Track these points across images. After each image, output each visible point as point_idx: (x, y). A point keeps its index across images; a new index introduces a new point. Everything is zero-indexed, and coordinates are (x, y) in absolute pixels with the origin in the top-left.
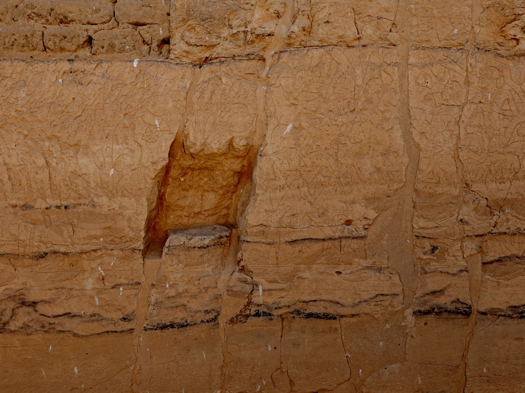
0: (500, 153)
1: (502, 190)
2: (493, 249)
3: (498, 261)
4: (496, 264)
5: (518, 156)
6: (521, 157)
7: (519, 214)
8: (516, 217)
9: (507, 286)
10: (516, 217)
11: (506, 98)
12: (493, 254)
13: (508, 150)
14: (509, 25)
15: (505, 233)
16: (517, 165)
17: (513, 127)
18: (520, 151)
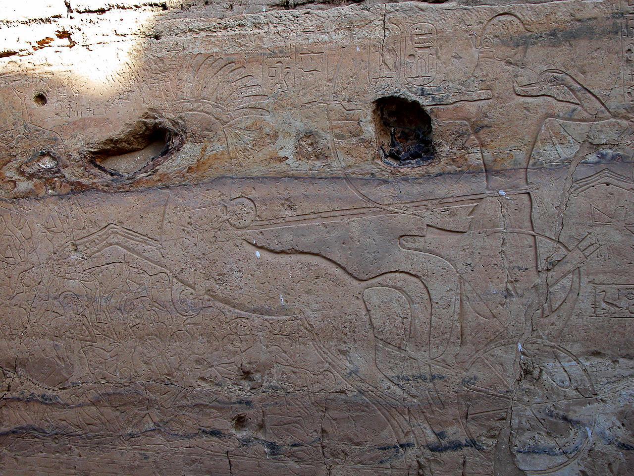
0: (6, 306)
1: (12, 348)
2: (8, 418)
3: (14, 432)
4: (11, 437)
5: (25, 310)
6: (28, 310)
7: (31, 376)
8: (30, 380)
9: (25, 463)
10: (30, 380)
11: (6, 244)
12: (8, 424)
13: (14, 301)
14: (5, 167)
15: (19, 400)
16: (25, 319)
17: (17, 276)
18: (27, 304)
